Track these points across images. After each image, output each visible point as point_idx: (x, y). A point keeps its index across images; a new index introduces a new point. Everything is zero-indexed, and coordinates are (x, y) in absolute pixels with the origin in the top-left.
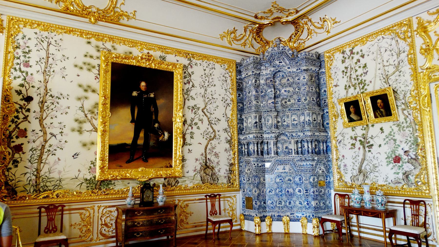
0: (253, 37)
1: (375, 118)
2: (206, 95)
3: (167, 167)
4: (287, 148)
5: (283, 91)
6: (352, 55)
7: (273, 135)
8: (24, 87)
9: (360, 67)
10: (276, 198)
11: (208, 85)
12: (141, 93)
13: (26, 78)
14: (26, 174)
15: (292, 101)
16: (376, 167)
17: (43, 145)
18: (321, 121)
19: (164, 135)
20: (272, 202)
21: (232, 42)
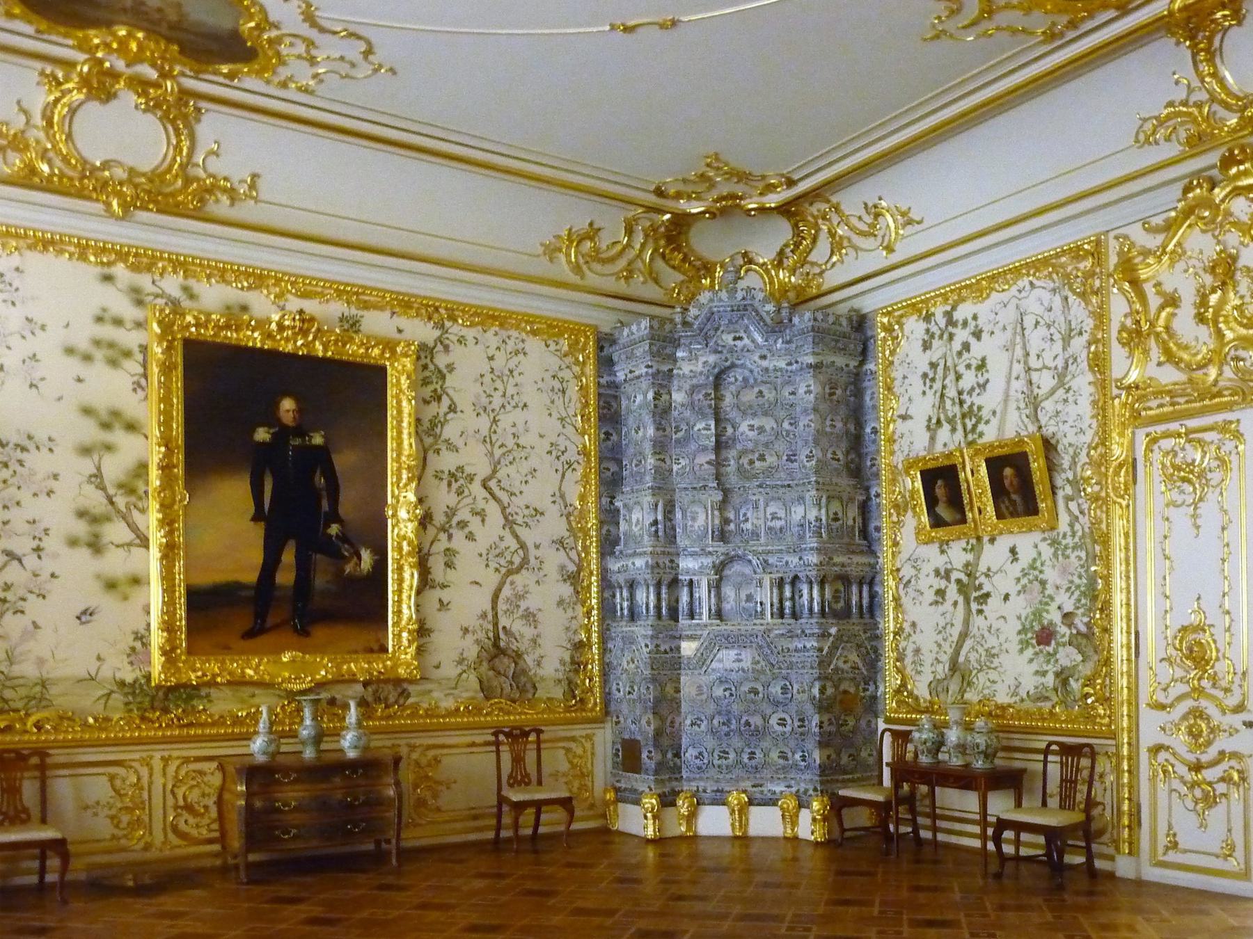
19: (359, 558)
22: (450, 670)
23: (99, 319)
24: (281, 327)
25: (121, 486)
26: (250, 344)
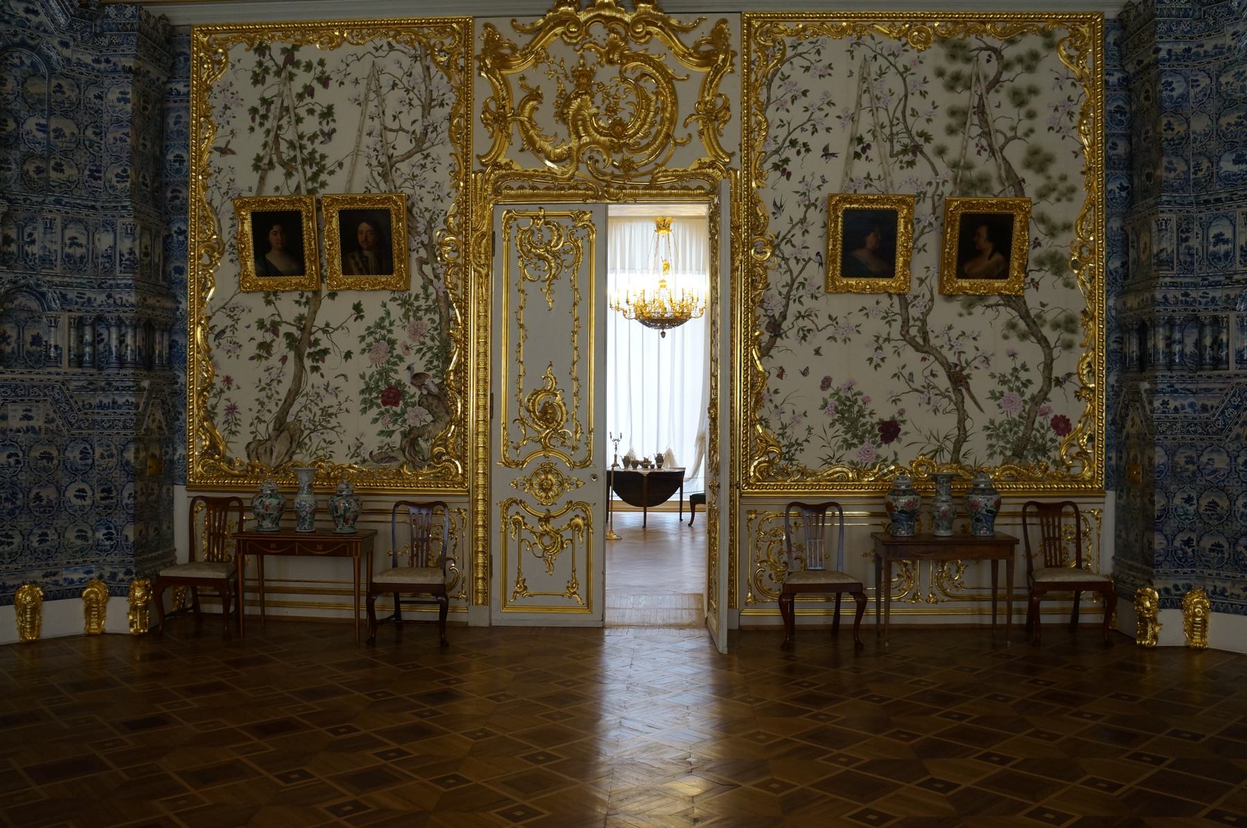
1: (344, 273)
4: (36, 340)
6: (289, 68)
9: (311, 112)
15: (70, 172)
16: (330, 415)
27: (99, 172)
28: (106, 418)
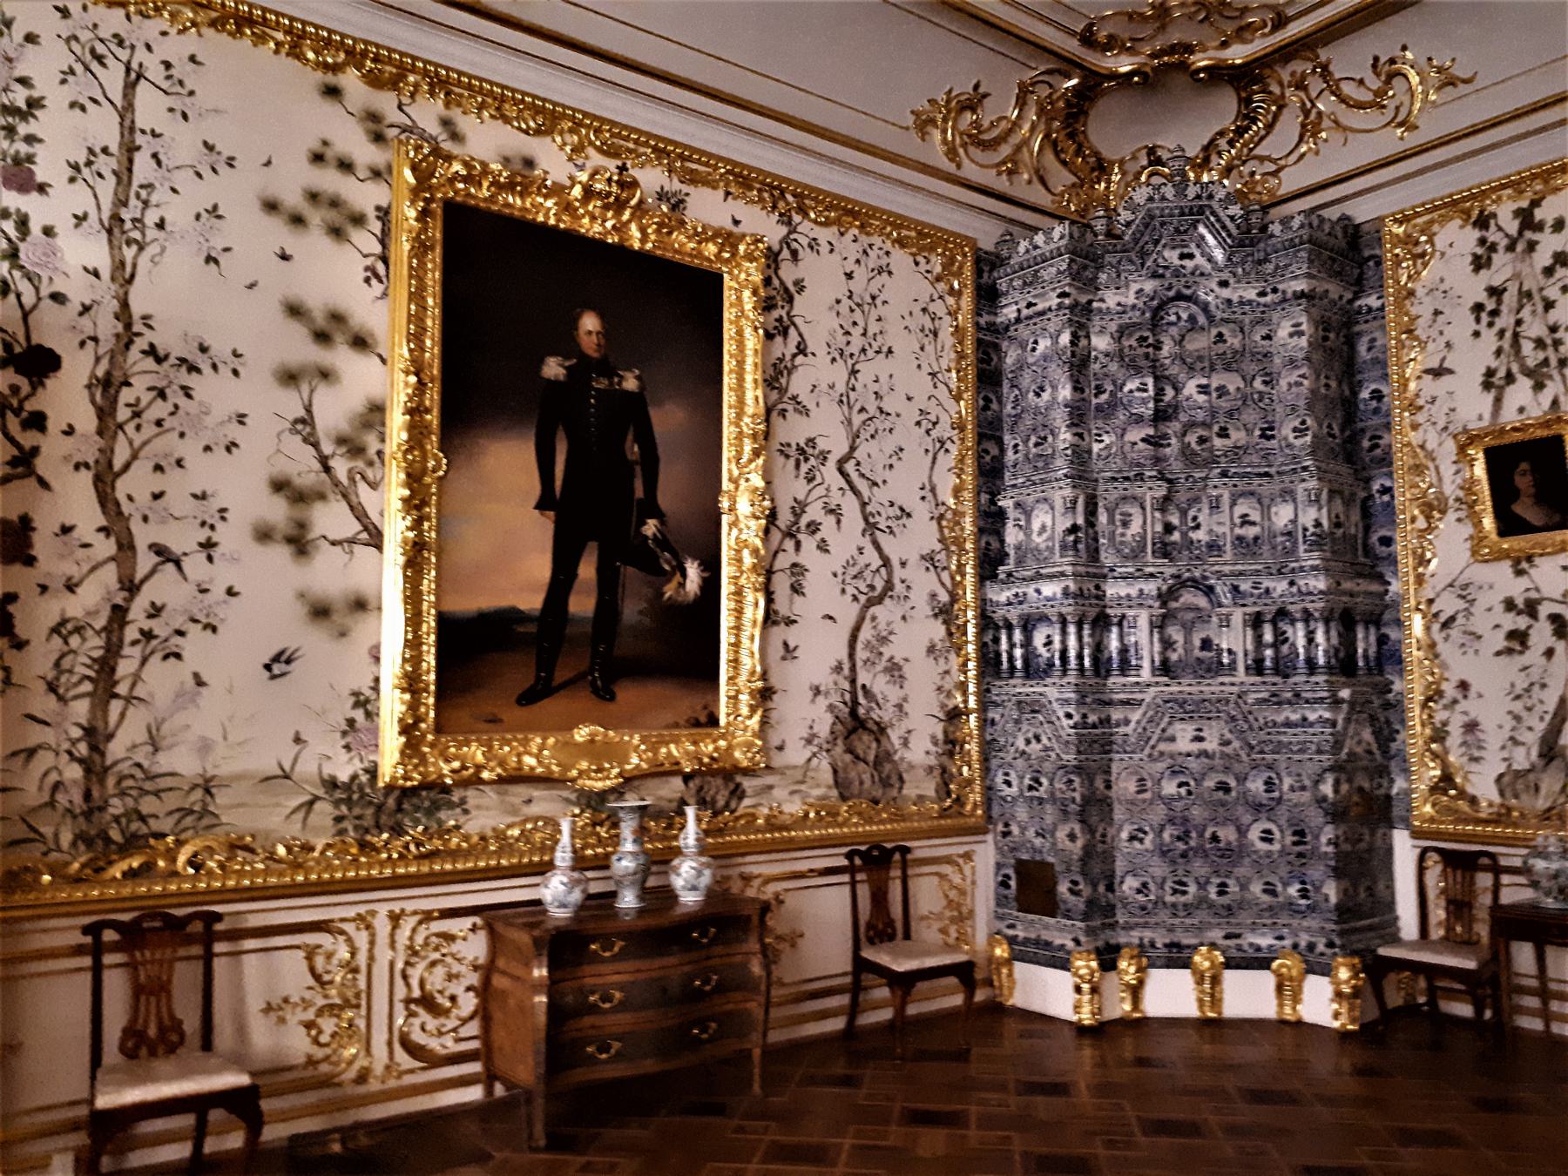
0: (1047, 136)
2: (852, 394)
3: (697, 724)
4: (1206, 644)
5: (1190, 388)
7: (1151, 587)
8: (12, 297)
10: (1159, 869)
11: (864, 350)
12: (583, 368)
13: (22, 246)
14: (31, 753)
15: (1237, 436)
17: (115, 608)
18: (1360, 525)
19: (684, 575)
20: (1145, 885)
21: (961, 151)
22: (796, 754)
23: (318, 158)
24: (589, 193)
25: (341, 441)
26: (541, 218)
27: (1272, 429)
28: (1294, 740)
